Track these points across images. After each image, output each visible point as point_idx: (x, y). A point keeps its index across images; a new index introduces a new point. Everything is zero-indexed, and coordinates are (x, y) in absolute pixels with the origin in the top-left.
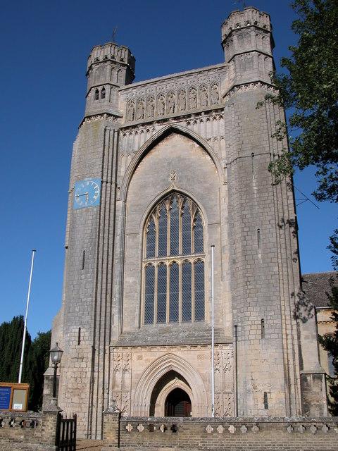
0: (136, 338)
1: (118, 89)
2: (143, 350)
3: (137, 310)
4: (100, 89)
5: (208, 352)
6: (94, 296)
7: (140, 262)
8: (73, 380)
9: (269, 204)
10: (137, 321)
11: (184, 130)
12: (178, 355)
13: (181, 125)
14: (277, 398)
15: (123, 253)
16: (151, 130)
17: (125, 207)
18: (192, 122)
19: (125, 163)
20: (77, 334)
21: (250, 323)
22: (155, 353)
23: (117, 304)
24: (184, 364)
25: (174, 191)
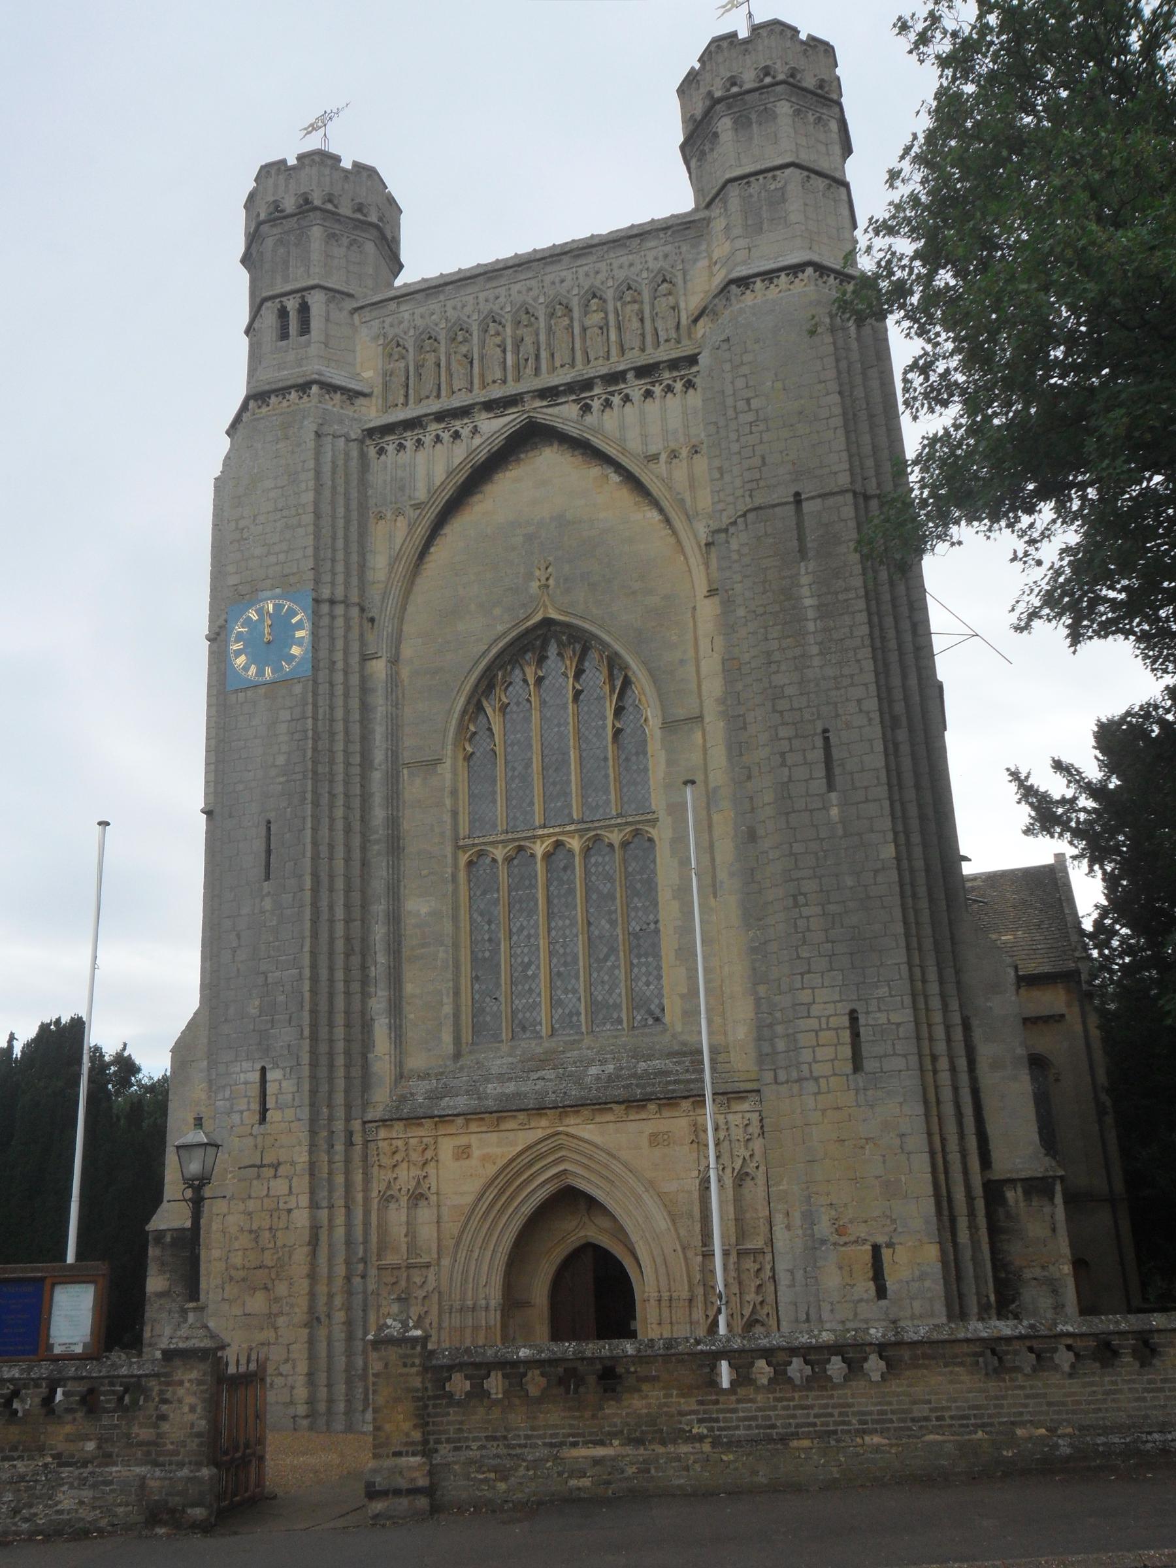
0: (448, 1092)
1: (350, 304)
2: (473, 1127)
3: (448, 1000)
4: (292, 304)
6: (306, 961)
7: (449, 850)
8: (245, 1240)
9: (855, 649)
10: (447, 1037)
11: (573, 430)
12: (586, 1136)
13: (564, 415)
14: (916, 1261)
15: (393, 822)
16: (465, 432)
17: (394, 681)
18: (596, 404)
19: (389, 540)
20: (255, 1091)
21: (813, 1023)
22: (511, 1135)
23: (382, 984)
25: (547, 622)
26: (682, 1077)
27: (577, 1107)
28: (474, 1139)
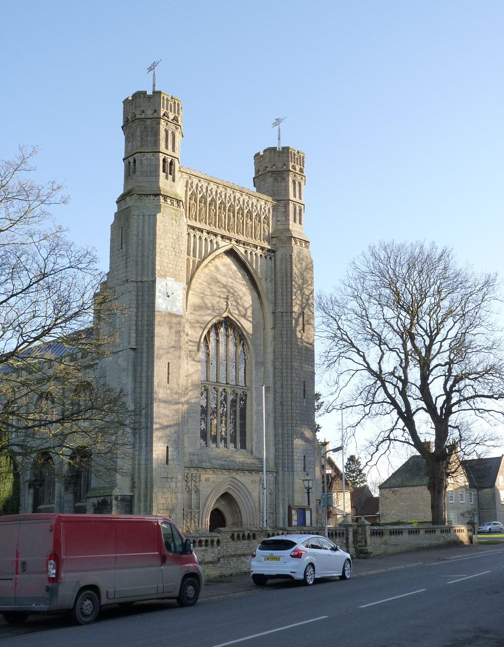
5: (258, 478)
24: (240, 487)
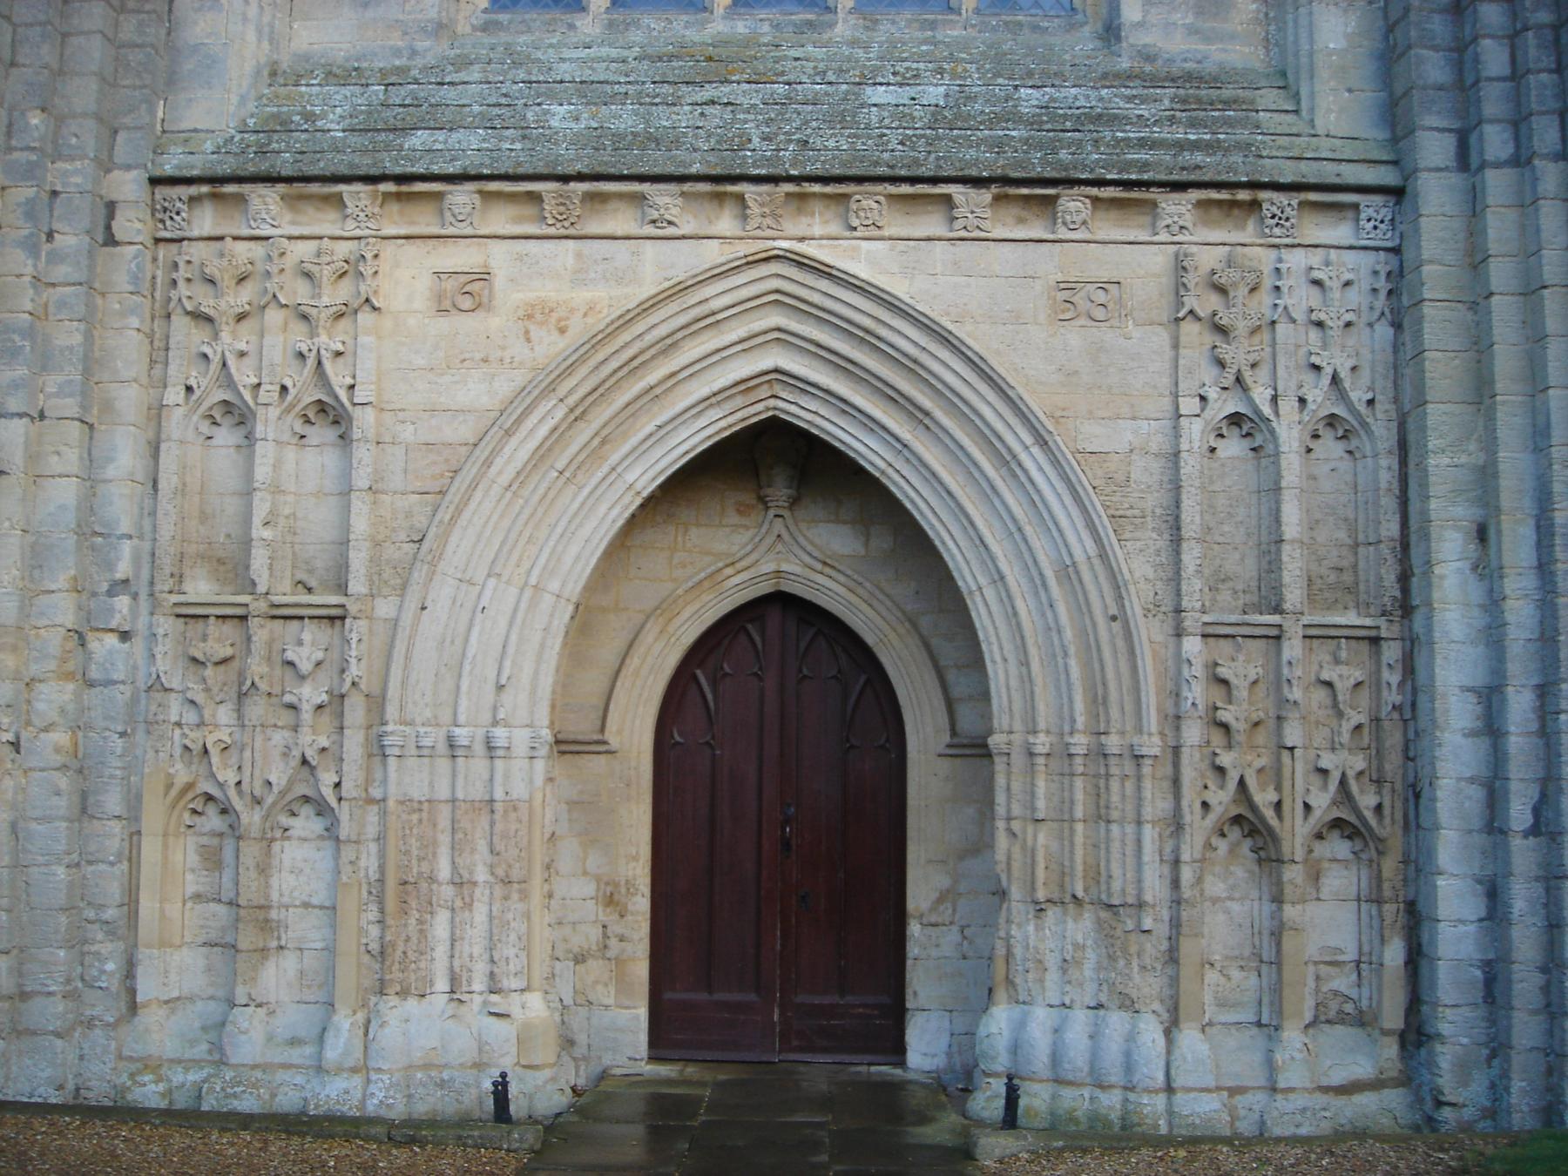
5: (1157, 260)
12: (860, 270)
24: (912, 367)
26: (1158, 133)
27: (836, 184)
28: (499, 256)
